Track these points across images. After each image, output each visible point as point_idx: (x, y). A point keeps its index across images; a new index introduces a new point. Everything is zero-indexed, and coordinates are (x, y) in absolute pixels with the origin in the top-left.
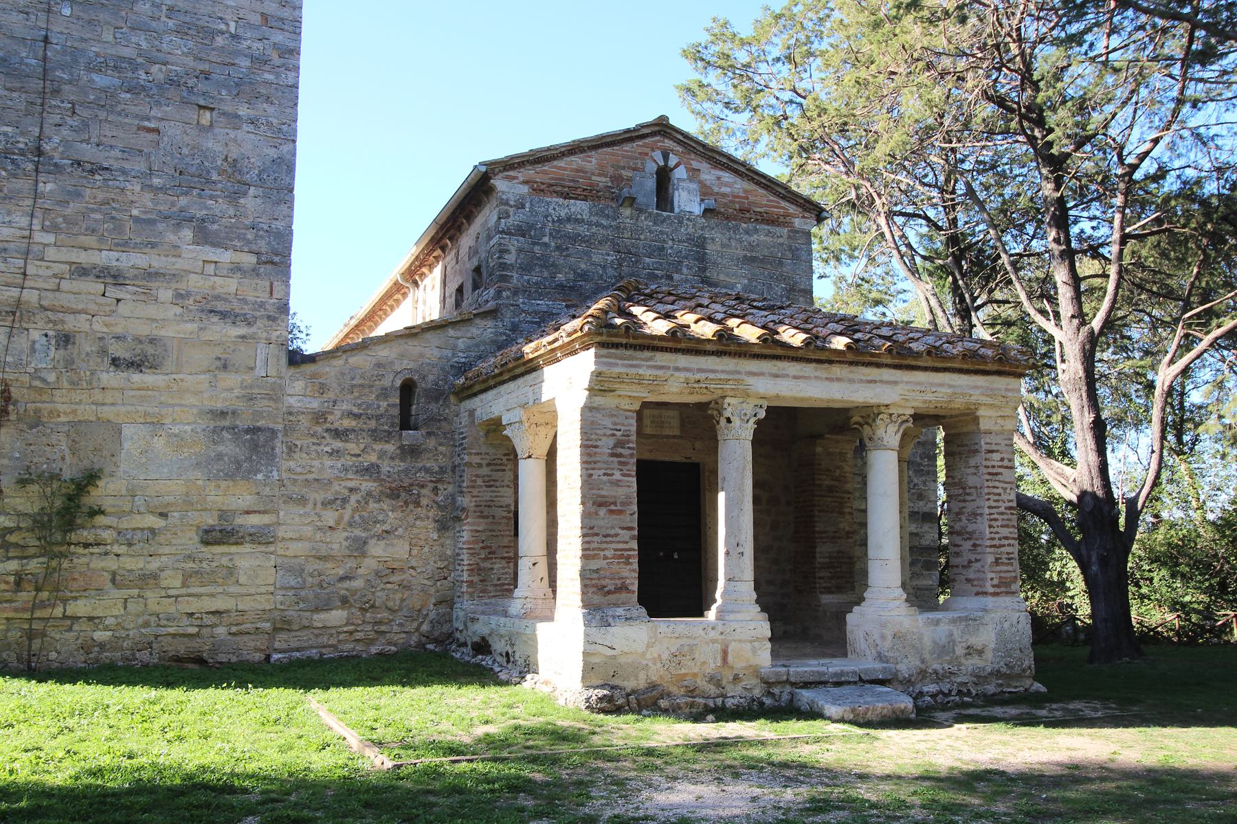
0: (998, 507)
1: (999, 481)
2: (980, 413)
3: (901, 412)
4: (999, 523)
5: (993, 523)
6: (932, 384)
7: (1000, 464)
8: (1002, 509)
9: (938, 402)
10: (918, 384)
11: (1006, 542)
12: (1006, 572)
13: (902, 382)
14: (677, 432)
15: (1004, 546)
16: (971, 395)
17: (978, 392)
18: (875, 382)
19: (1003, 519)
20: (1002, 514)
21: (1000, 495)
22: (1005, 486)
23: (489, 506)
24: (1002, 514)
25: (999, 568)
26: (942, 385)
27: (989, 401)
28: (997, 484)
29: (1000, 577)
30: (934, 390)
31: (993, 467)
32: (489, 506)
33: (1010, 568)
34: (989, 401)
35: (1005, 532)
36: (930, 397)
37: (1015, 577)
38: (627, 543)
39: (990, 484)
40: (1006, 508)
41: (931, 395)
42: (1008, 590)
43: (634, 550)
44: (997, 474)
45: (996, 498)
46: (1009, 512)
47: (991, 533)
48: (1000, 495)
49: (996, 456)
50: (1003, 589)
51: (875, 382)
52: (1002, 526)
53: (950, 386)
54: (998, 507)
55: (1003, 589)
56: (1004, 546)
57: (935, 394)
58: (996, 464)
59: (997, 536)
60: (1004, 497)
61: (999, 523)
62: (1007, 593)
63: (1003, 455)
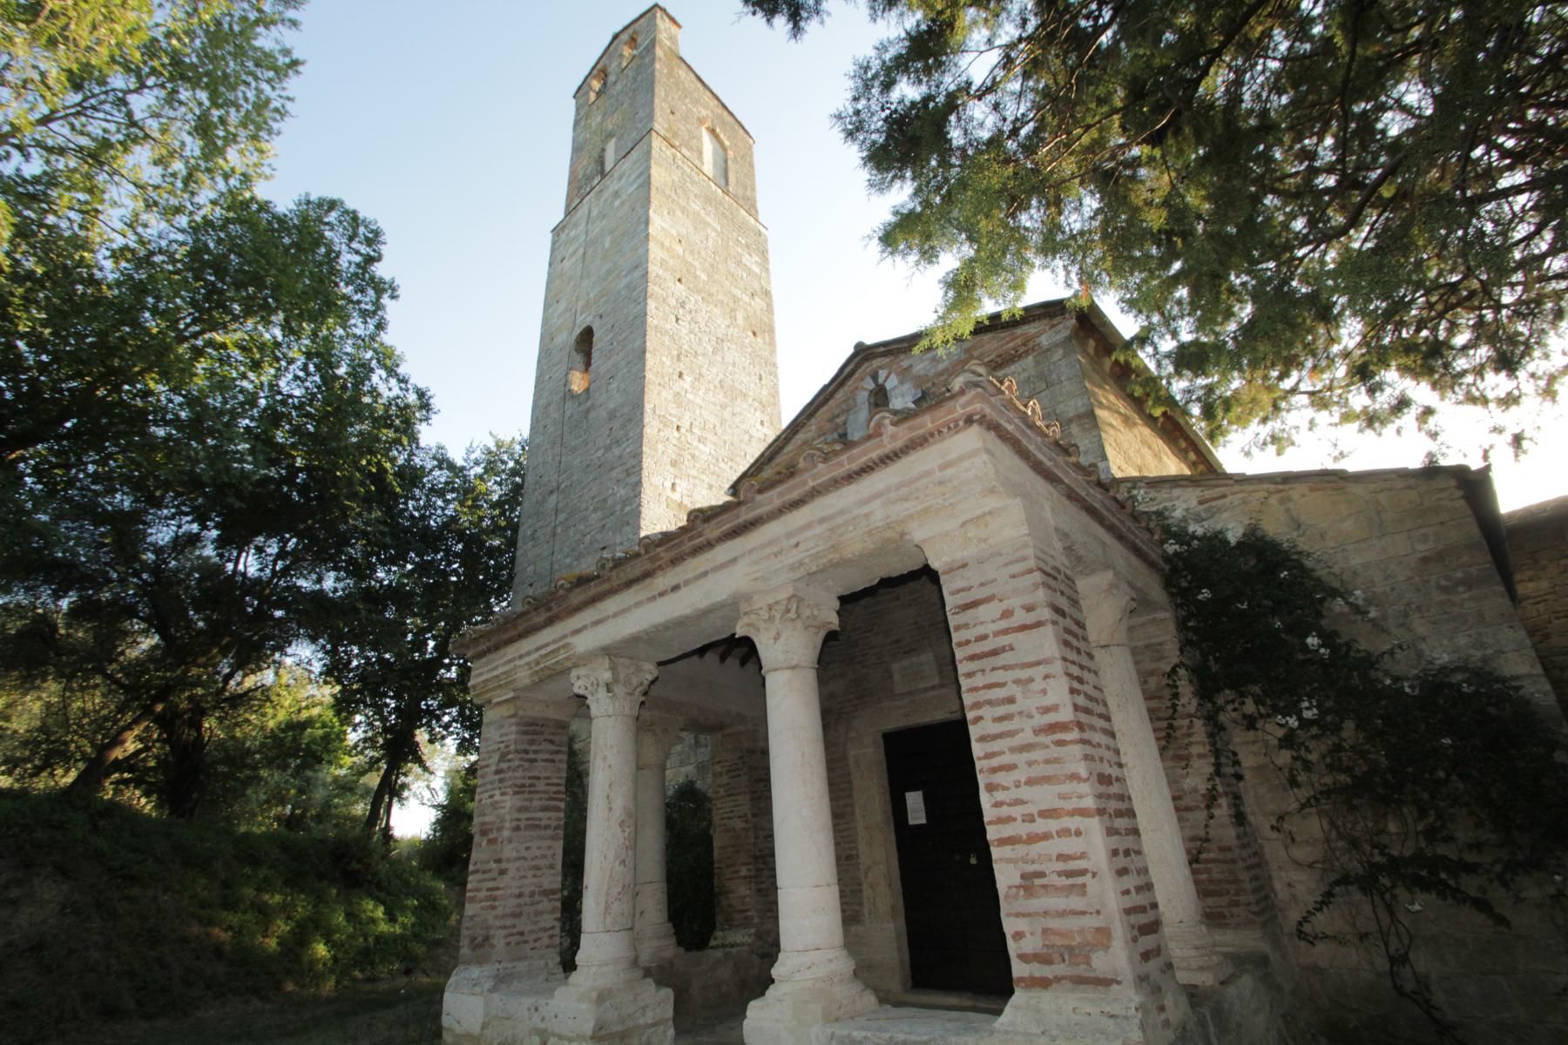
0: (1010, 734)
1: (1005, 668)
2: (918, 534)
3: (771, 600)
4: (1021, 775)
5: (1000, 778)
6: (789, 535)
7: (1003, 624)
8: (1027, 737)
9: (816, 557)
10: (770, 543)
11: (1052, 825)
12: (1063, 914)
13: (743, 555)
14: (936, 681)
15: (1046, 837)
16: (867, 516)
17: (877, 504)
18: (705, 574)
19: (1030, 764)
20: (1028, 748)
21: (1011, 700)
22: (1024, 674)
23: (730, 818)
24: (1028, 748)
25: (1035, 904)
26: (808, 526)
27: (911, 507)
28: (999, 676)
29: (1045, 931)
30: (793, 541)
31: (984, 637)
32: (730, 818)
33: (1076, 902)
34: (911, 507)
35: (1044, 797)
36: (794, 556)
37: (1104, 932)
38: (494, 879)
39: (979, 680)
40: (1037, 732)
41: (795, 552)
42: (1081, 970)
43: (1003, 842)
44: (994, 653)
45: (1000, 711)
46: (1047, 739)
47: (998, 805)
48: (1011, 700)
49: (984, 612)
50: (1058, 969)
51: (705, 574)
52: (1030, 782)
53: (821, 521)
54: (1010, 734)
55: (1058, 969)
56: (1046, 837)
57: (801, 548)
58: (989, 629)
59: (1017, 811)
60: (1023, 703)
61: (1021, 775)
62: (1079, 981)
63: (1005, 605)
